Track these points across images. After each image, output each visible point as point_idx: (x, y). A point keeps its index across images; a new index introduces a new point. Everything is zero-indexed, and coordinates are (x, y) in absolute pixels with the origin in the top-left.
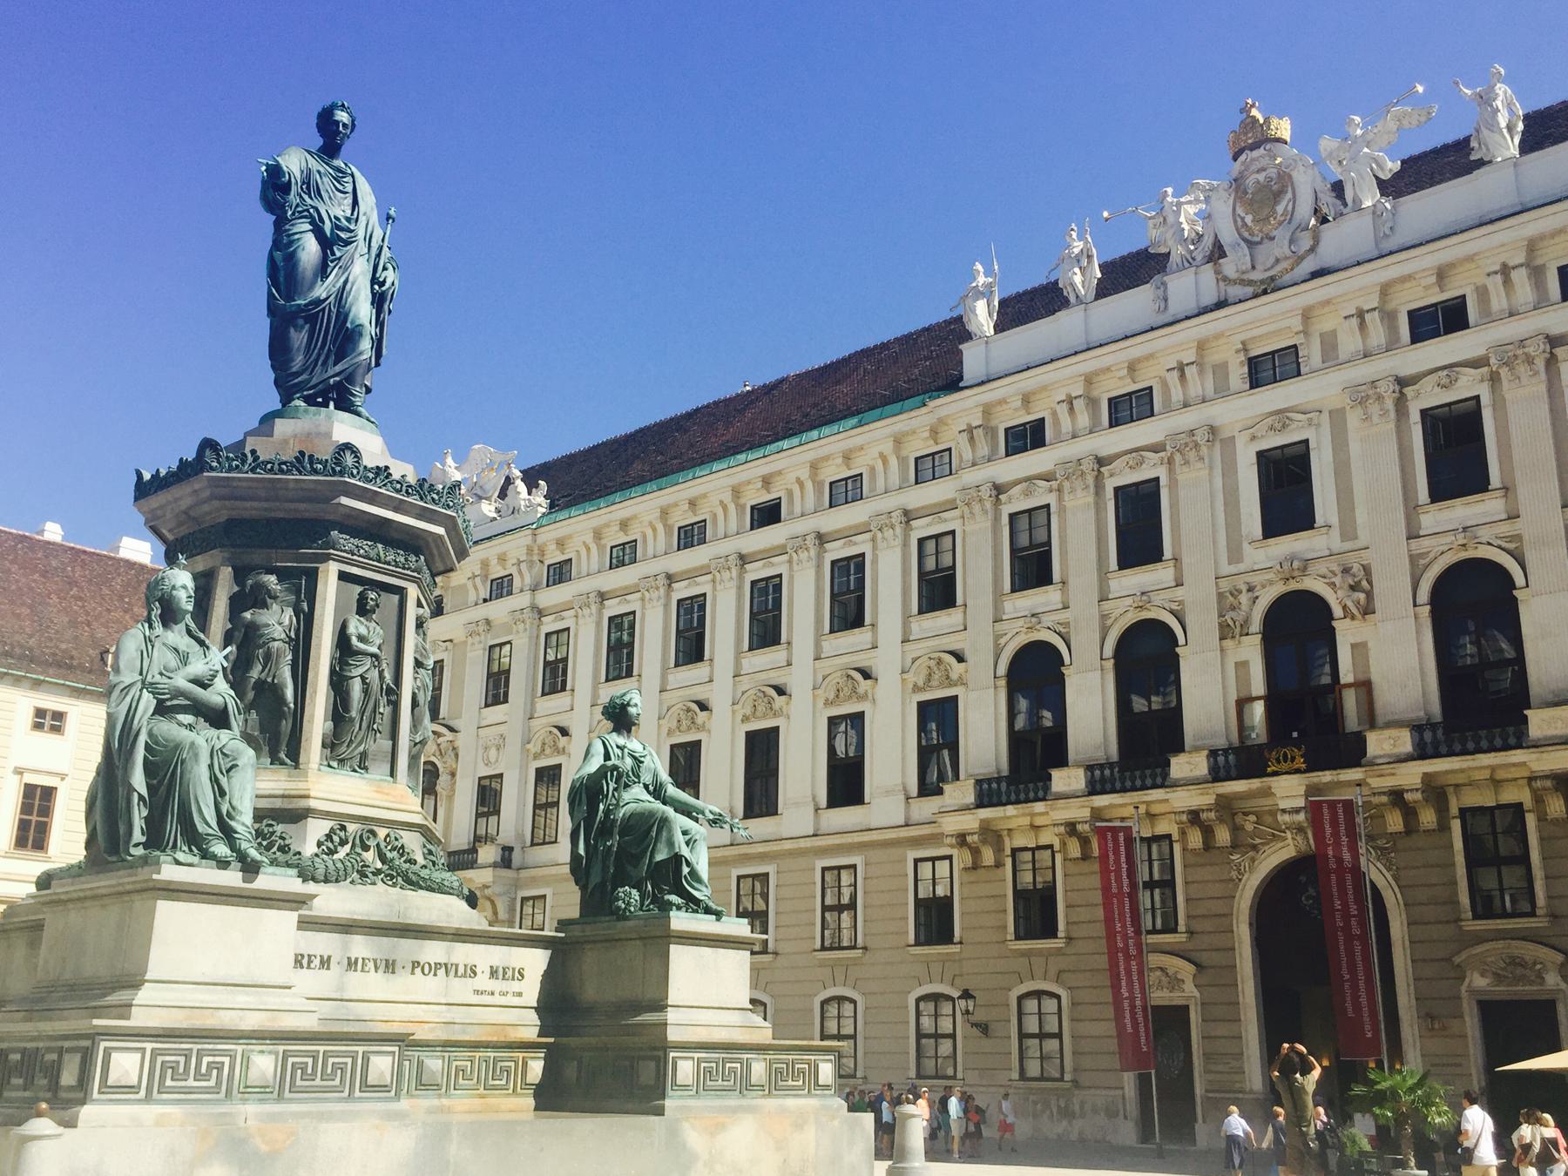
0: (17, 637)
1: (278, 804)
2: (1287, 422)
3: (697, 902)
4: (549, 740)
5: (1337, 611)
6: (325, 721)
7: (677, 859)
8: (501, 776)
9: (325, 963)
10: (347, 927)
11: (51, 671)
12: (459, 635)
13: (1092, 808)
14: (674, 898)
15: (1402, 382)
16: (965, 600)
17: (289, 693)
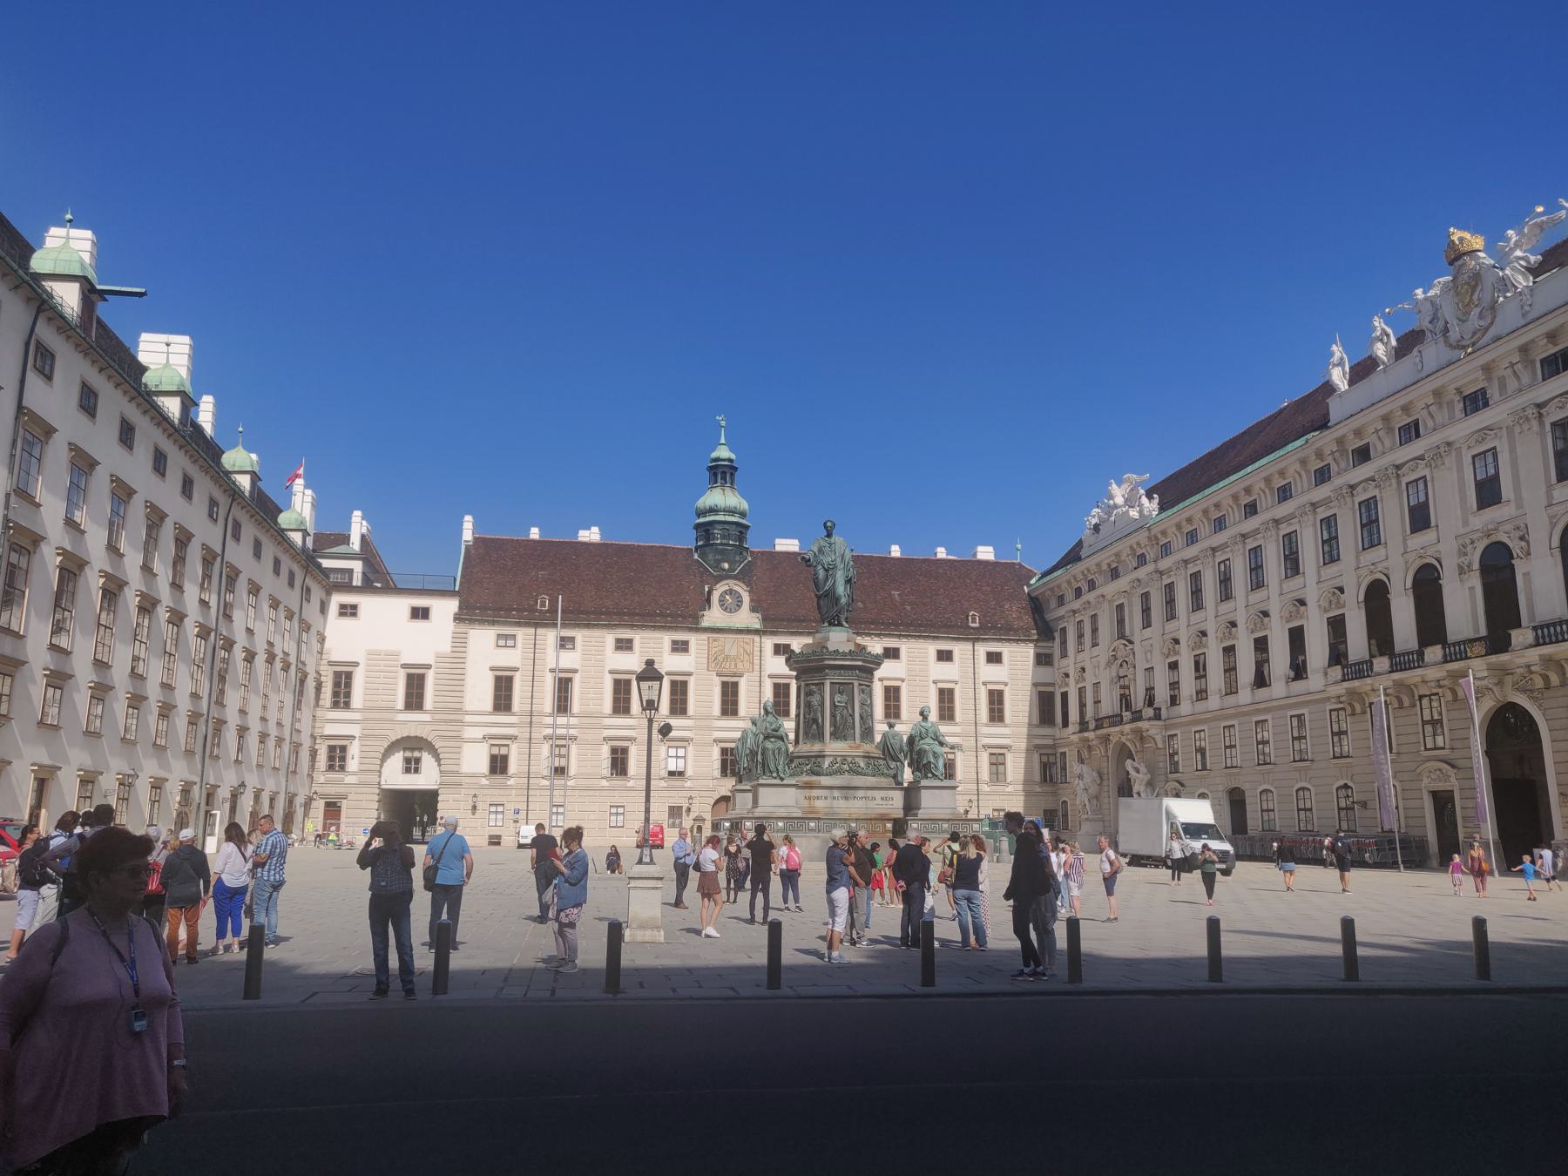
0: (924, 615)
1: (817, 754)
2: (1485, 436)
3: (936, 776)
4: (1171, 646)
5: (1515, 556)
6: (830, 727)
7: (930, 762)
8: (1152, 668)
9: (826, 798)
10: (831, 788)
11: (942, 630)
12: (1127, 588)
13: (1393, 681)
14: (930, 775)
15: (1540, 406)
16: (1437, 522)
17: (820, 721)
